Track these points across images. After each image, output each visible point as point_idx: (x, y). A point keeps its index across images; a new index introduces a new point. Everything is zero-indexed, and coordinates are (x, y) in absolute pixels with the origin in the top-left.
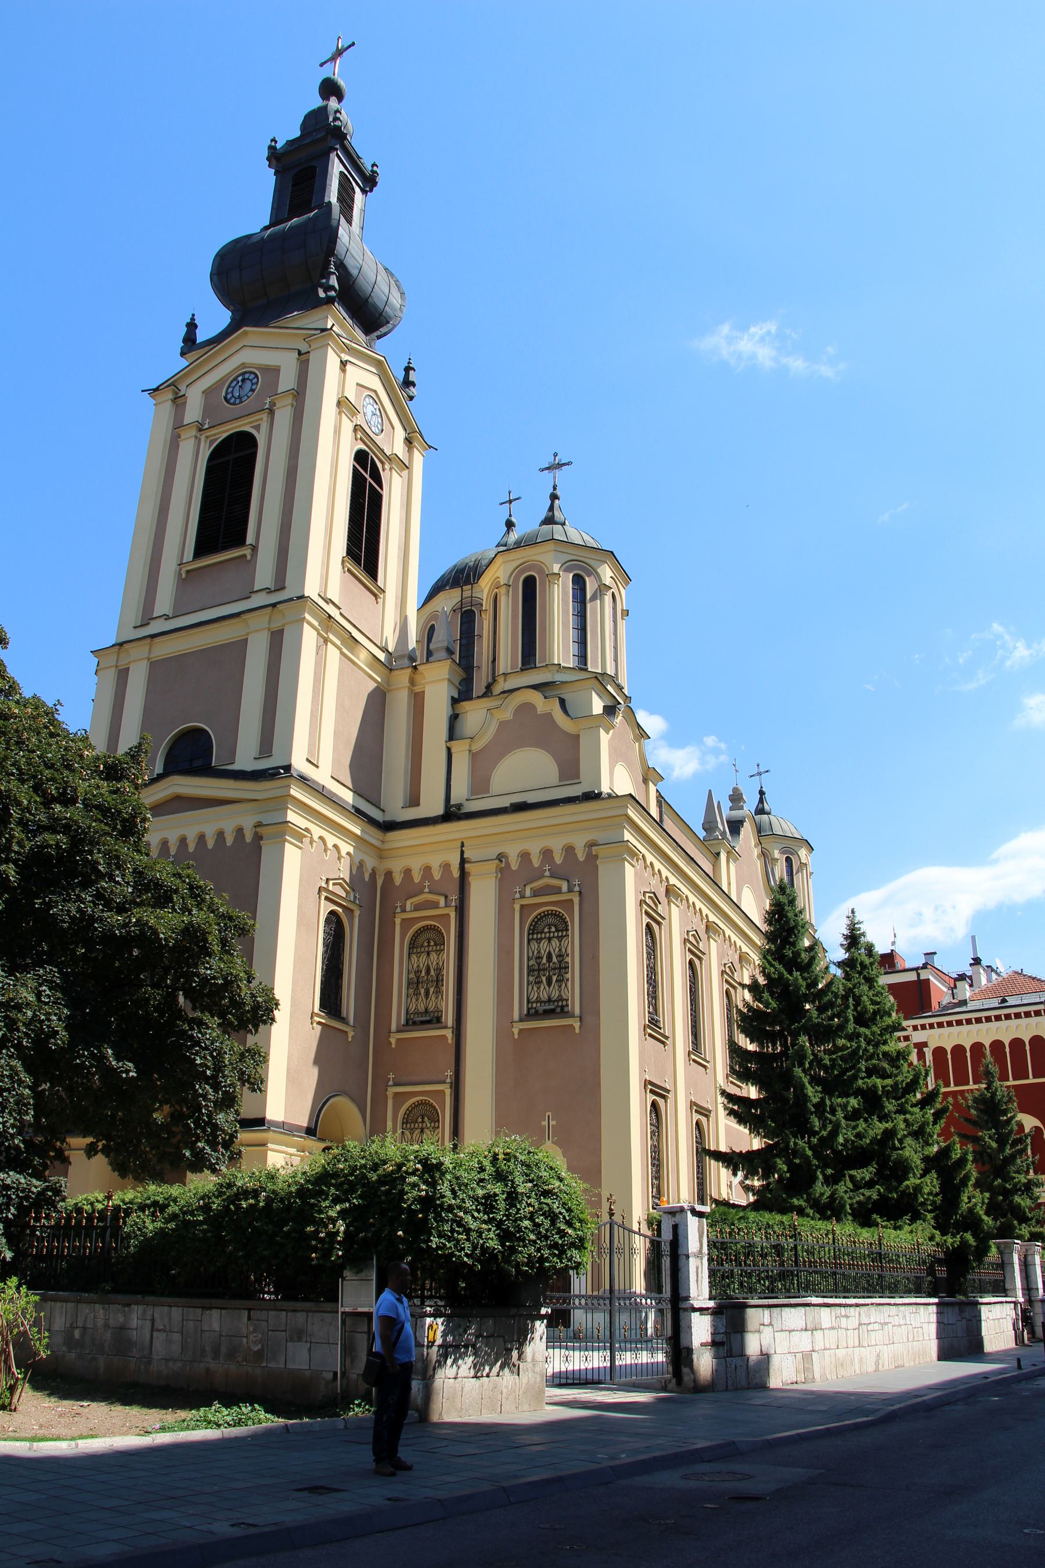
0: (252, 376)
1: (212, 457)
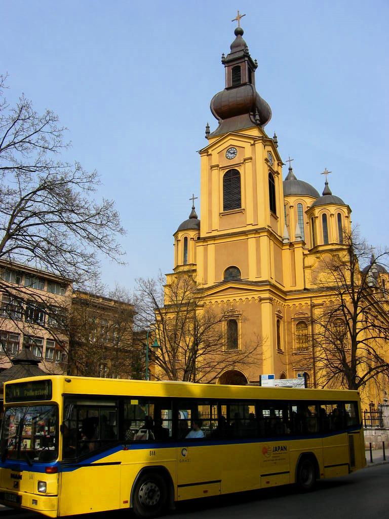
0: (234, 150)
1: (225, 175)
